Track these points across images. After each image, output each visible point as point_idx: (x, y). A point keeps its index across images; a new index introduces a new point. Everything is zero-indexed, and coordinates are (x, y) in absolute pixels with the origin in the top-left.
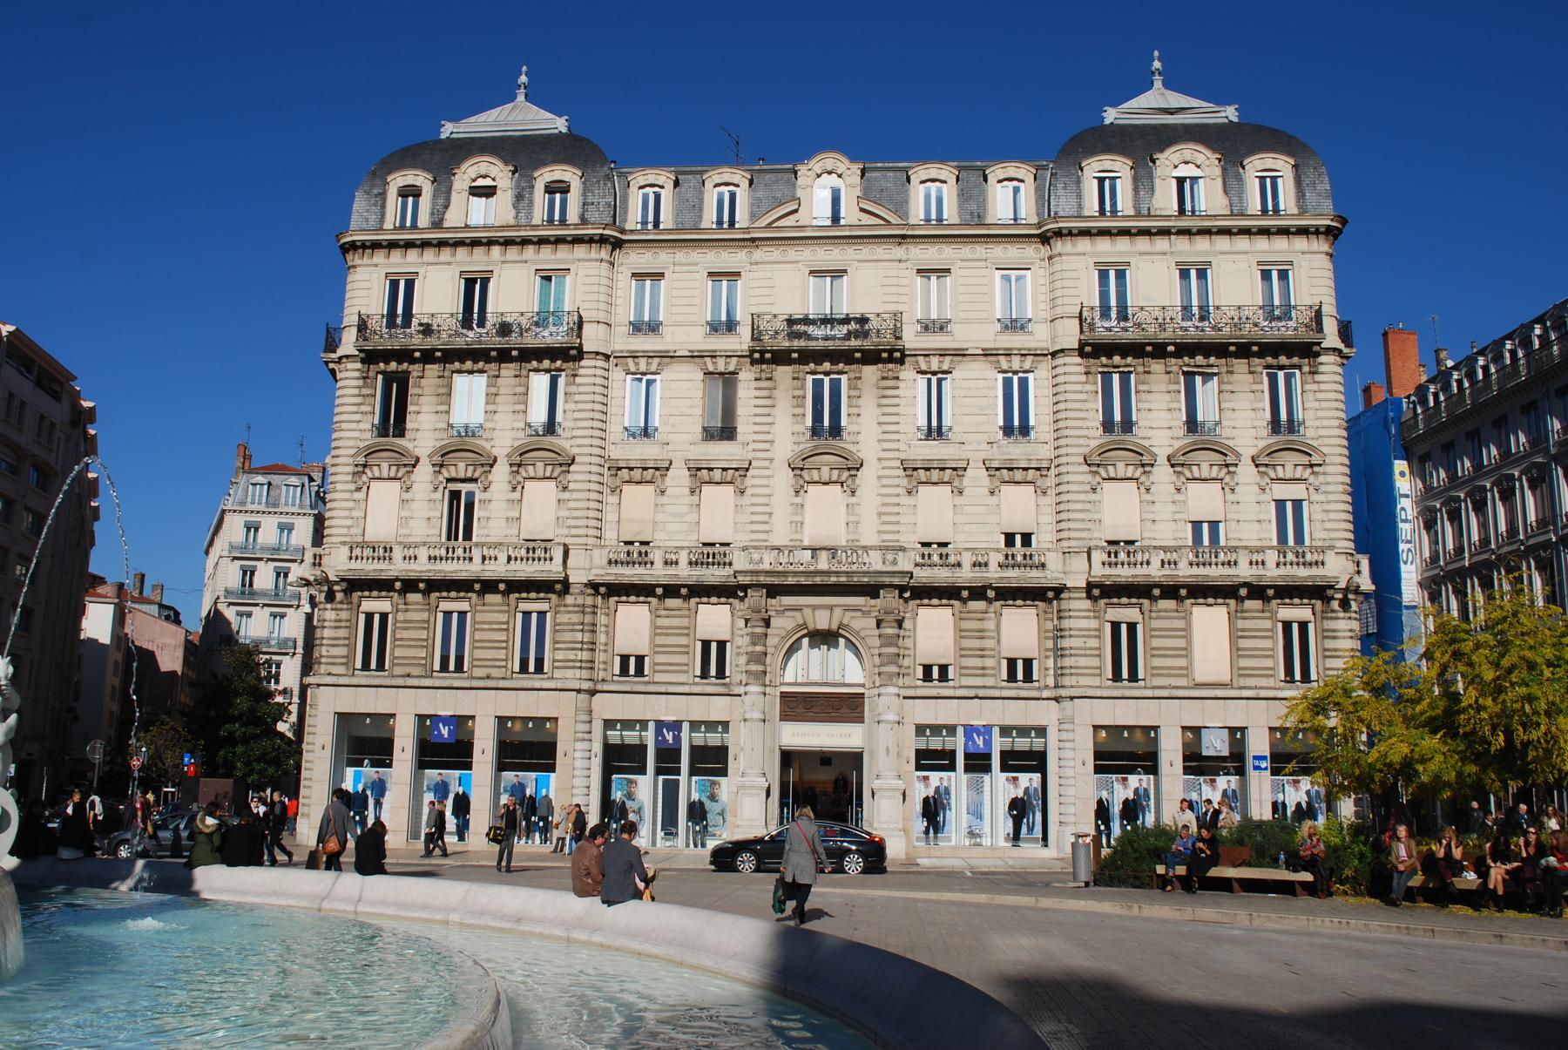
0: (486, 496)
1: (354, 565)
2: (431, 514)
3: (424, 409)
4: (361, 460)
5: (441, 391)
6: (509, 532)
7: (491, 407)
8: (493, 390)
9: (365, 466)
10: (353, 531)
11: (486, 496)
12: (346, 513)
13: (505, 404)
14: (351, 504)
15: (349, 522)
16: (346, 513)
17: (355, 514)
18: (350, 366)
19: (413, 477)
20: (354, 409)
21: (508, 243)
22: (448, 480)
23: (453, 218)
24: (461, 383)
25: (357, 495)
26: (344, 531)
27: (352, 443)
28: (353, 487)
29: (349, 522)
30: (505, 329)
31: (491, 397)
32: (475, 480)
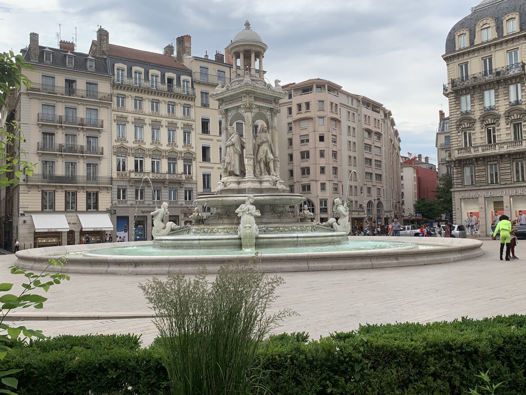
0: (499, 128)
1: (460, 155)
2: (482, 136)
3: (476, 104)
4: (458, 123)
5: (480, 97)
6: (508, 138)
7: (497, 100)
8: (497, 94)
9: (460, 125)
10: (459, 145)
11: (499, 128)
12: (456, 140)
13: (501, 98)
14: (457, 137)
15: (457, 142)
16: (456, 140)
17: (459, 140)
18: (451, 95)
19: (475, 126)
20: (455, 108)
21: (495, 45)
22: (486, 125)
23: (477, 41)
24: (486, 93)
25: (459, 134)
26: (456, 145)
27: (455, 119)
28: (457, 132)
29: (457, 142)
30: (498, 73)
31: (496, 96)
32: (494, 124)
